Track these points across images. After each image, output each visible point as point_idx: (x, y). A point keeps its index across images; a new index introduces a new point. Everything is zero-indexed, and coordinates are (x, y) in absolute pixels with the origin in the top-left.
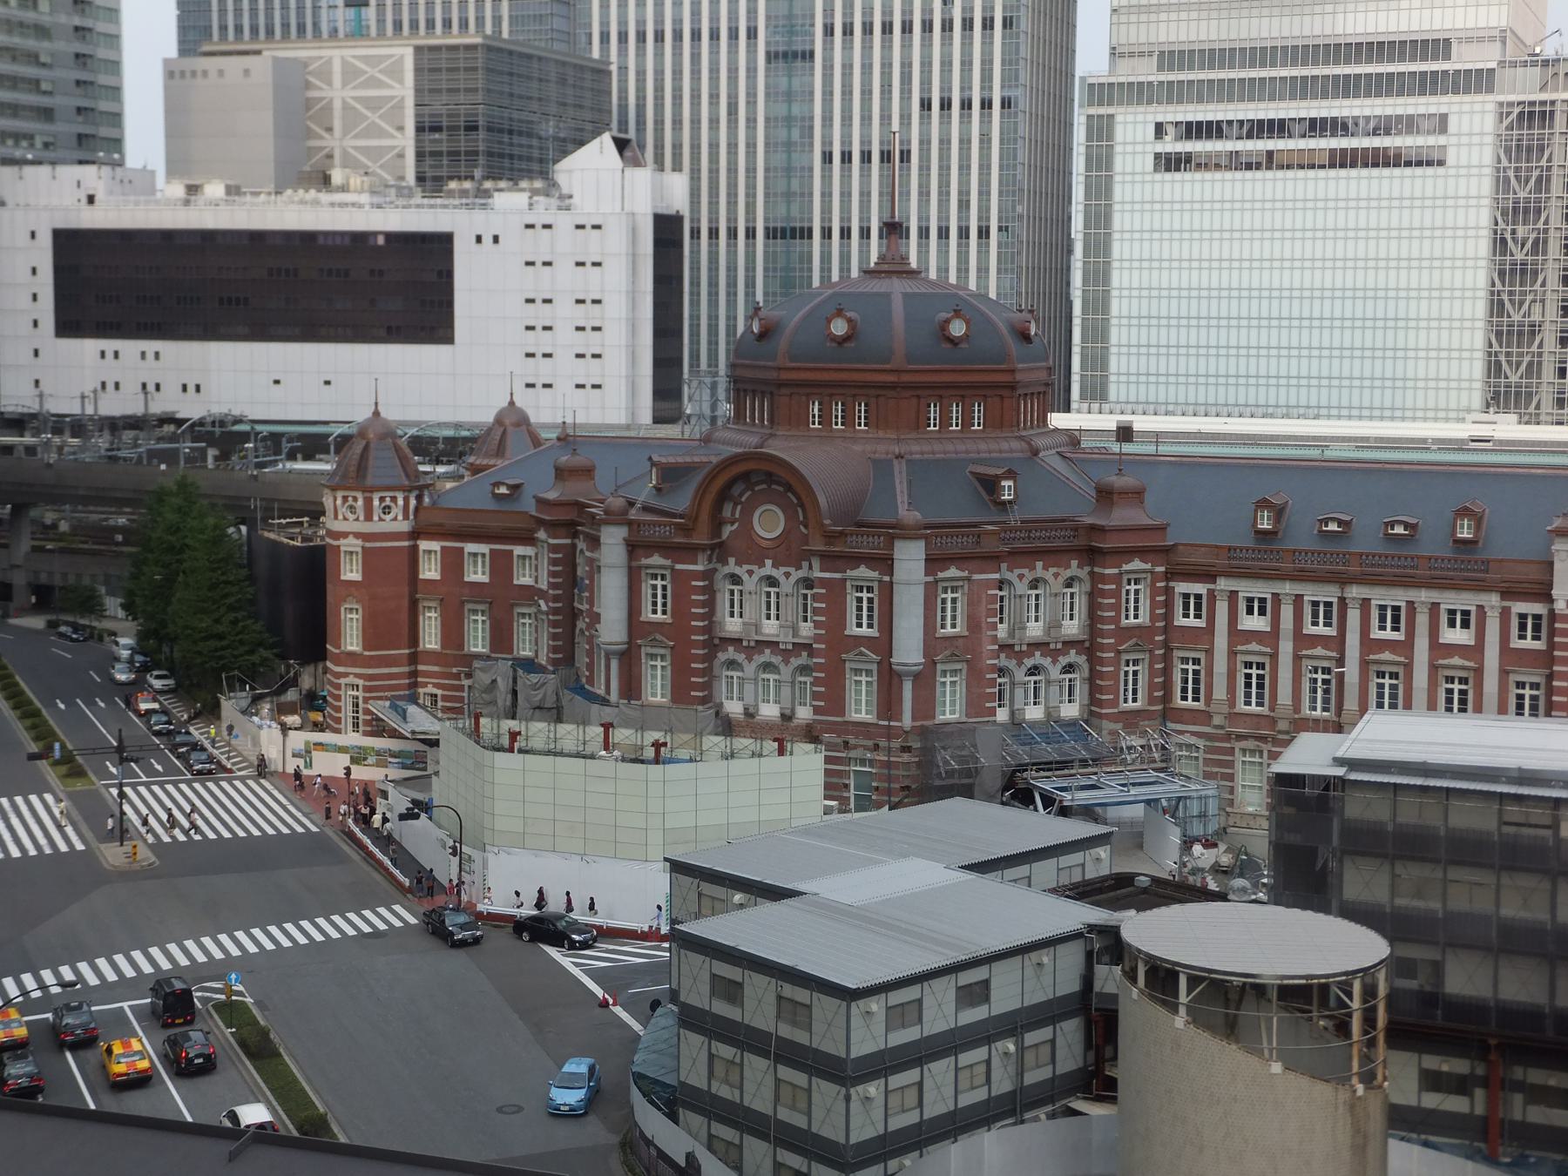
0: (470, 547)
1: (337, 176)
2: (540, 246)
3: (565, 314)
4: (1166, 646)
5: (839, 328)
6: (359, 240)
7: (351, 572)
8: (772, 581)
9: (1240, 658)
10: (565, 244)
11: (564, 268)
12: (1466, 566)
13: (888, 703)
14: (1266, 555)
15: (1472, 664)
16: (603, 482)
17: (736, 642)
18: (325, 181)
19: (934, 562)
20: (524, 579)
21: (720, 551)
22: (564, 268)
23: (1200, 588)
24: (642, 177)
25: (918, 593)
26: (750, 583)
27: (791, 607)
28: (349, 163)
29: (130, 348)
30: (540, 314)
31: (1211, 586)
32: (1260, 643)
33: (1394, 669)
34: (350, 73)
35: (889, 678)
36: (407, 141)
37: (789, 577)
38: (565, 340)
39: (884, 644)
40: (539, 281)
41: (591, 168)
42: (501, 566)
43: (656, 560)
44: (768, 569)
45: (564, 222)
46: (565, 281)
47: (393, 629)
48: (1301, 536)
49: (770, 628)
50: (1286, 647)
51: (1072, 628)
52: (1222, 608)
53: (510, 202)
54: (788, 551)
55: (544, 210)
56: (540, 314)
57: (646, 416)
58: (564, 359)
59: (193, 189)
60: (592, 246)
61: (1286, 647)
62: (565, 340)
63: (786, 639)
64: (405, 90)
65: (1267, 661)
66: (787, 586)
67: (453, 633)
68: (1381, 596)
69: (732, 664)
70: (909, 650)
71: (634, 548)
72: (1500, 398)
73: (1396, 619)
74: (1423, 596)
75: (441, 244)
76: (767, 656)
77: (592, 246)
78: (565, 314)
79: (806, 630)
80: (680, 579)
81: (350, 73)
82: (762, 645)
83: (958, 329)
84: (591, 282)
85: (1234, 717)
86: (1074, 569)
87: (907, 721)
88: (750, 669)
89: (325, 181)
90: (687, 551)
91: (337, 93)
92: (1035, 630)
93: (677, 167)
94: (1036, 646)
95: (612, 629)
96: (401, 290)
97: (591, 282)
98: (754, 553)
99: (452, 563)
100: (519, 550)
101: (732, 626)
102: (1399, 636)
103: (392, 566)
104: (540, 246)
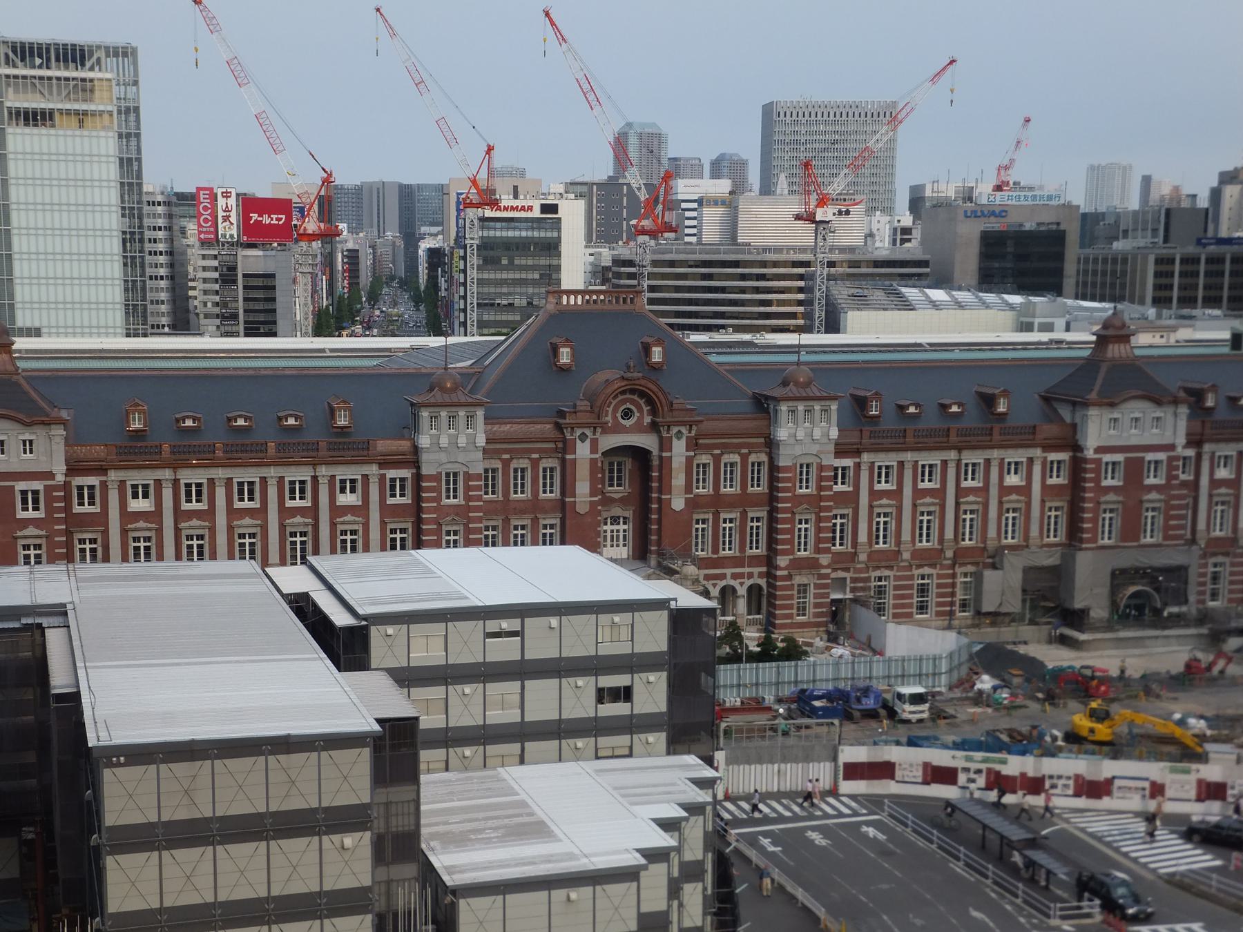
4: (69, 533)
9: (132, 534)
15: (43, 533)
31: (104, 478)
32: (932, 497)
33: (38, 541)
65: (152, 534)
72: (137, 318)
73: (199, 493)
102: (203, 506)
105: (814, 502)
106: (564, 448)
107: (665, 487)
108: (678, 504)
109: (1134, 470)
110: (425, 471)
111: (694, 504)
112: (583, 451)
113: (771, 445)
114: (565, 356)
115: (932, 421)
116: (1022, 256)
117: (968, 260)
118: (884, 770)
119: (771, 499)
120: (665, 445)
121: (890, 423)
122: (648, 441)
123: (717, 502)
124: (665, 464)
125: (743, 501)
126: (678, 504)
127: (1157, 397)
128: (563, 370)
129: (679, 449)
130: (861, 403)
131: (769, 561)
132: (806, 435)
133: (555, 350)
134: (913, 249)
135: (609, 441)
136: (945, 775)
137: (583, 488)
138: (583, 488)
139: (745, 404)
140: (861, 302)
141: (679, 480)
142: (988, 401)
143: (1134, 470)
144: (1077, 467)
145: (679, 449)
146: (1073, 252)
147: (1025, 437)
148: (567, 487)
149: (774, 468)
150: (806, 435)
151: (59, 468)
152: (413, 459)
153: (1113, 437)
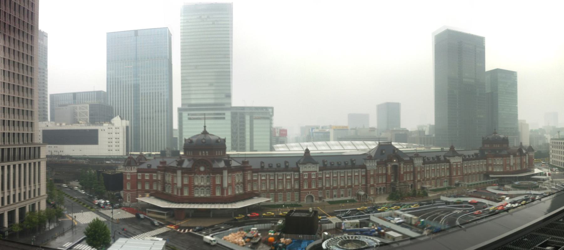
0: (146, 174)
1: (80, 122)
2: (111, 131)
3: (114, 140)
5: (204, 141)
6: (85, 130)
7: (128, 178)
8: (202, 177)
10: (114, 130)
11: (114, 134)
12: (287, 169)
13: (222, 193)
14: (262, 169)
16: (167, 163)
17: (197, 186)
18: (78, 123)
19: (228, 173)
20: (155, 178)
21: (195, 173)
22: (114, 134)
23: (256, 174)
24: (124, 121)
25: (227, 177)
26: (199, 177)
27: (205, 181)
28: (80, 120)
29: (53, 146)
30: (110, 140)
34: (80, 108)
35: (222, 190)
36: (88, 117)
37: (205, 177)
38: (114, 144)
39: (221, 185)
40: (110, 136)
41: (117, 120)
42: (151, 177)
43: (186, 175)
44: (202, 175)
45: (114, 128)
46: (114, 135)
47: (134, 187)
48: (266, 166)
49: (202, 184)
50: (268, 181)
51: (241, 180)
52: (259, 177)
53: (106, 125)
54: (204, 173)
55: (110, 126)
56: (110, 140)
57: (125, 154)
58: (114, 147)
59: (61, 124)
60: (118, 131)
61: (268, 181)
62: (114, 144)
63: (205, 185)
64: (88, 110)
66: (205, 178)
67: (143, 187)
68: (279, 173)
69: (197, 189)
70: (225, 185)
71: (182, 173)
74: (284, 173)
75: (96, 131)
76: (202, 188)
77: (118, 131)
78: (114, 140)
79: (208, 184)
80: (190, 177)
81: (80, 108)
82: (201, 186)
83: (219, 141)
84: (118, 136)
85: (262, 190)
86: (241, 173)
87: (225, 195)
88: (200, 190)
89: (78, 123)
90: (191, 173)
91: (78, 111)
92: (237, 181)
93: (129, 120)
94: (238, 183)
95: (179, 185)
96: (91, 137)
97: (118, 136)
98: (200, 173)
99: (143, 176)
100: (154, 174)
101: (196, 184)
103: (134, 177)
104: (111, 131)
106: (386, 165)
107: (400, 170)
108: (402, 173)
109: (457, 165)
110: (368, 169)
111: (404, 173)
112: (389, 166)
114: (384, 152)
120: (400, 164)
123: (406, 173)
124: (400, 167)
125: (410, 172)
126: (402, 173)
127: (459, 156)
128: (383, 154)
129: (402, 165)
131: (414, 181)
132: (418, 162)
133: (382, 151)
135: (393, 164)
137: (389, 171)
138: (389, 171)
141: (402, 169)
144: (450, 165)
145: (402, 165)
148: (387, 171)
149: (414, 168)
151: (318, 170)
153: (454, 161)
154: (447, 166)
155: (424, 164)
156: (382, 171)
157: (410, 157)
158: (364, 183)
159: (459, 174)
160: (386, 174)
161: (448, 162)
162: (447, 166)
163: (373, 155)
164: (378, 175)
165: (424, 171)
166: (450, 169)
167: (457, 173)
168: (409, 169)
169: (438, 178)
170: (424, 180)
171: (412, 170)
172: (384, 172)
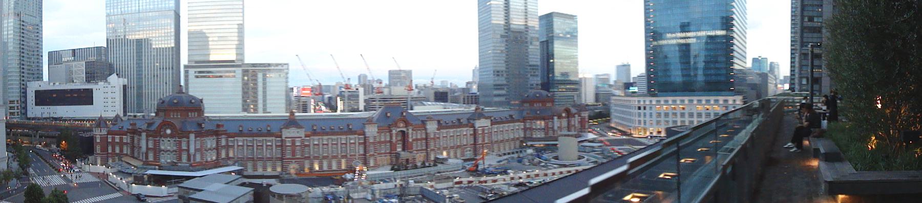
105: (433, 139)
112: (394, 132)
113: (426, 129)
115: (450, 124)
116: (441, 96)
117: (432, 97)
118: (460, 183)
119: (426, 139)
121: (444, 124)
122: (404, 129)
123: (417, 140)
125: (421, 139)
127: (487, 118)
129: (410, 131)
130: (439, 121)
132: (432, 127)
134: (422, 95)
136: (470, 182)
139: (420, 123)
140: (416, 105)
142: (459, 120)
143: (483, 130)
146: (449, 96)
147: (466, 126)
149: (427, 134)
150: (432, 127)
152: (364, 134)
154: (471, 131)
155: (438, 129)
156: (385, 137)
157: (423, 121)
158: (362, 152)
159: (486, 141)
160: (390, 142)
161: (473, 126)
162: (471, 131)
163: (375, 120)
164: (380, 142)
165: (439, 138)
166: (475, 134)
167: (484, 140)
168: (420, 135)
169: (458, 147)
170: (439, 149)
171: (424, 136)
172: (388, 139)
